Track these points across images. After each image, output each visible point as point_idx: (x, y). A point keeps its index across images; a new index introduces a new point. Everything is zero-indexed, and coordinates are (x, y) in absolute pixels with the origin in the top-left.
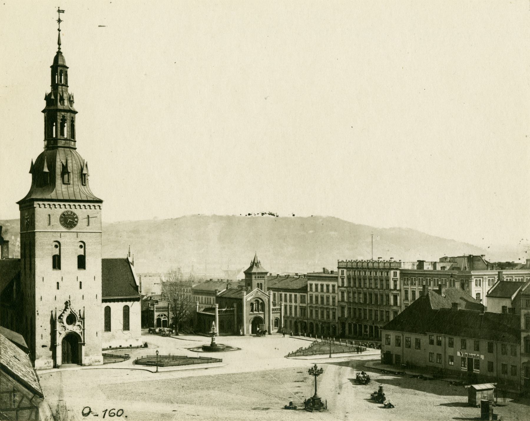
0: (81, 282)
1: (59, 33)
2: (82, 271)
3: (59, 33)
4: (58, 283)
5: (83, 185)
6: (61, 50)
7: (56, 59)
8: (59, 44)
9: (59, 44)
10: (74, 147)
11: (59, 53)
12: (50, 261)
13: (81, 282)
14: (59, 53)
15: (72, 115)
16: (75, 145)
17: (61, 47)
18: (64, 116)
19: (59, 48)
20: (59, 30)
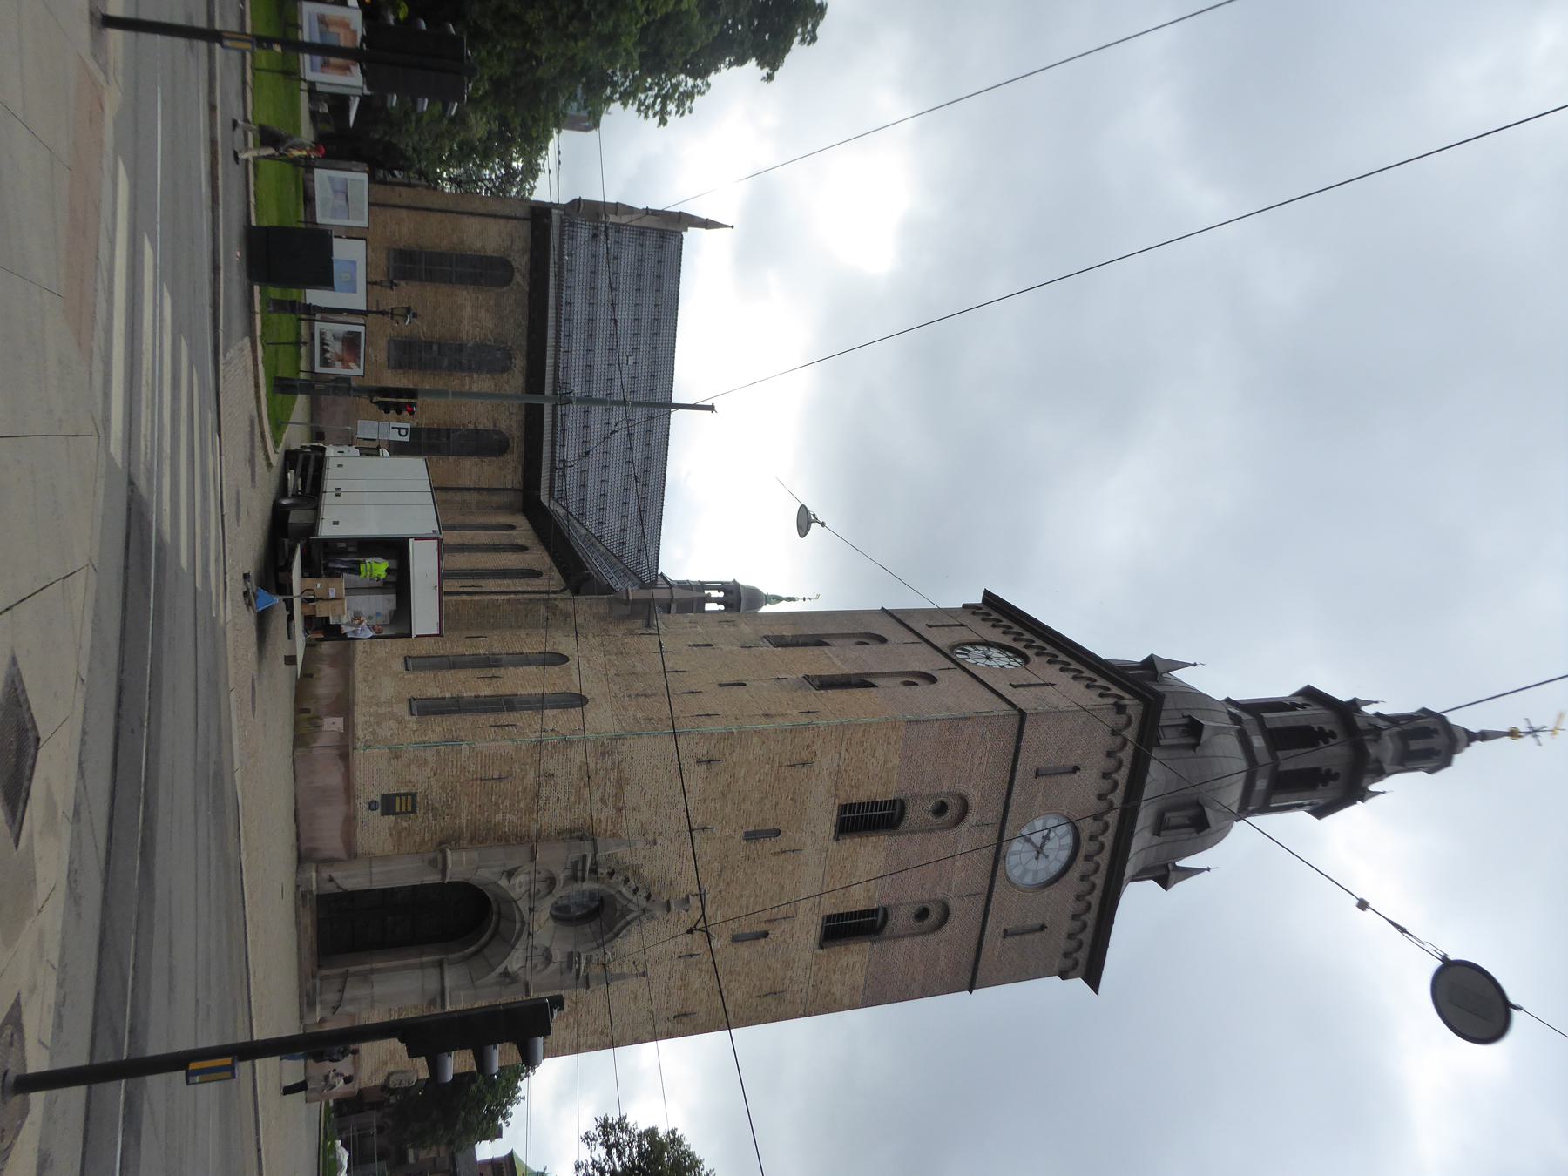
4: (777, 833)
8: (1484, 736)
9: (1484, 736)
13: (766, 935)
20: (1513, 734)
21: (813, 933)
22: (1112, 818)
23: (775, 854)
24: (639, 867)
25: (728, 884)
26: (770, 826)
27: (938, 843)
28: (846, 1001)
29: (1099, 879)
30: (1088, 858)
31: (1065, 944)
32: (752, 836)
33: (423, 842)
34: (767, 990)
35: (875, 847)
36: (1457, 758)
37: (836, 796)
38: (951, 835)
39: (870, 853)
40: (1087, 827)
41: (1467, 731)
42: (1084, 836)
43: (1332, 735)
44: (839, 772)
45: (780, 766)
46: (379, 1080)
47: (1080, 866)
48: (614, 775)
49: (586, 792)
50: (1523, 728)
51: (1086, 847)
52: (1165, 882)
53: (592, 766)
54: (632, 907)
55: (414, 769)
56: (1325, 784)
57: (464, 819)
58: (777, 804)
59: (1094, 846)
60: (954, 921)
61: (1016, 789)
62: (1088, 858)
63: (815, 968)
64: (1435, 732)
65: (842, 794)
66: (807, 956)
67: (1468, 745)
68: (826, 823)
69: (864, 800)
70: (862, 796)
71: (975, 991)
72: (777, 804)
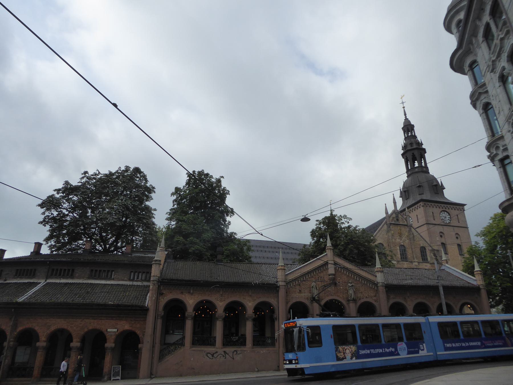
1: (404, 109)
3: (404, 109)
6: (407, 118)
8: (405, 114)
9: (405, 114)
14: (406, 119)
17: (407, 116)
19: (406, 117)
20: (404, 107)
22: (439, 205)
29: (449, 206)
30: (446, 209)
36: (412, 124)
41: (405, 120)
42: (443, 209)
43: (413, 154)
47: (447, 210)
50: (402, 106)
51: (444, 209)
52: (444, 188)
59: (444, 207)
64: (408, 128)
67: (408, 119)
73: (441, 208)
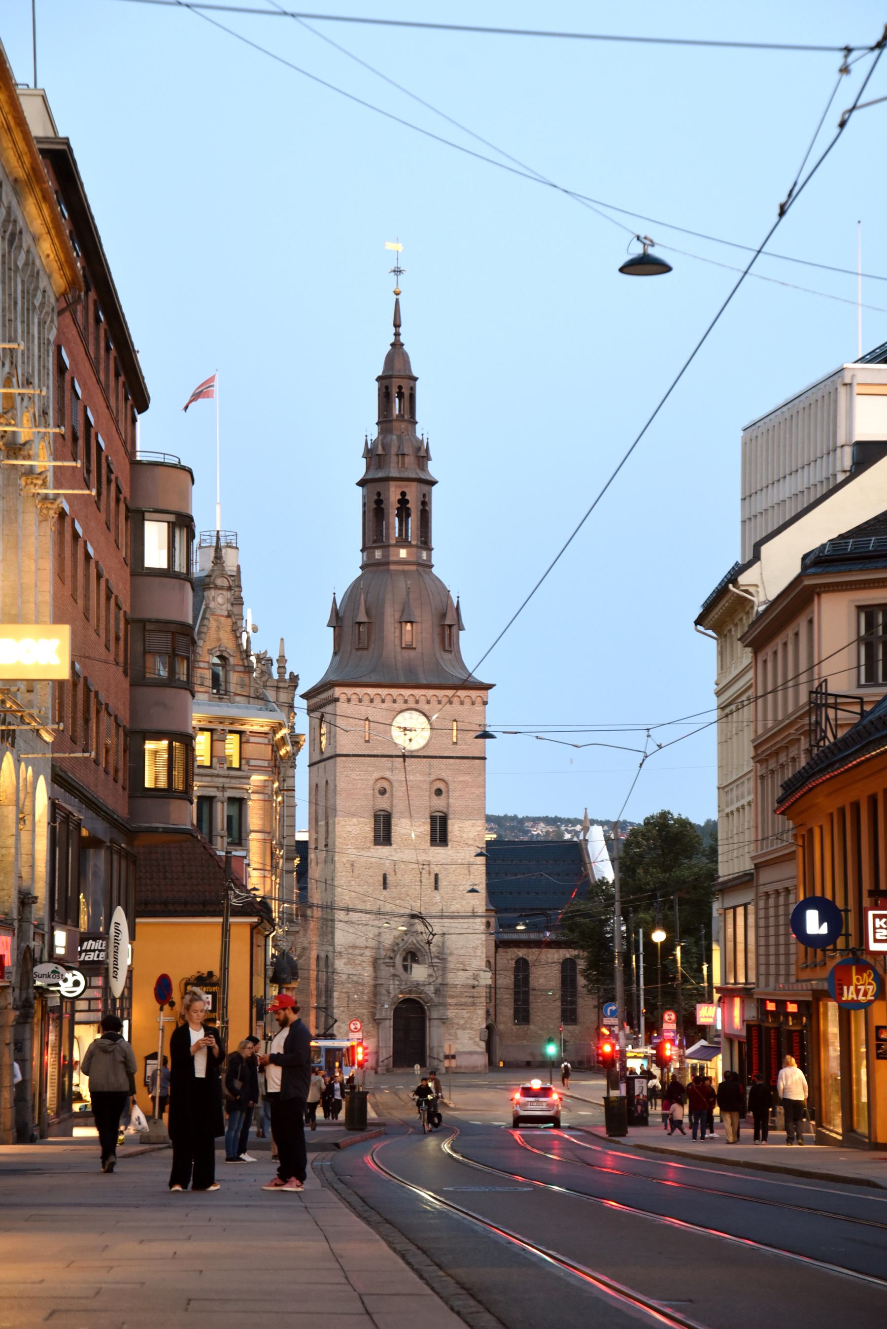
0: (436, 875)
2: (439, 852)
5: (445, 650)
6: (402, 339)
7: (390, 360)
8: (397, 325)
9: (397, 325)
10: (427, 563)
11: (397, 345)
12: (365, 827)
13: (436, 875)
14: (397, 345)
15: (425, 488)
16: (429, 557)
17: (401, 330)
18: (403, 494)
19: (397, 334)
21: (438, 851)
23: (395, 874)
24: (395, 937)
25: (408, 895)
26: (381, 879)
27: (399, 791)
28: (479, 829)
31: (467, 706)
32: (385, 885)
33: (373, 1027)
34: (467, 871)
35: (396, 825)
37: (369, 848)
38: (395, 784)
39: (401, 827)
40: (400, 705)
41: (392, 345)
42: (405, 706)
44: (357, 848)
45: (352, 877)
46: (483, 1044)
48: (350, 951)
49: (357, 962)
51: (411, 704)
53: (345, 960)
54: (410, 941)
55: (341, 1031)
56: (407, 502)
57: (365, 1011)
58: (371, 876)
60: (443, 775)
61: (375, 752)
62: (417, 702)
63: (458, 847)
65: (368, 845)
66: (450, 852)
68: (383, 851)
69: (373, 834)
70: (371, 835)
71: (487, 757)
72: (371, 876)
73: (400, 700)
